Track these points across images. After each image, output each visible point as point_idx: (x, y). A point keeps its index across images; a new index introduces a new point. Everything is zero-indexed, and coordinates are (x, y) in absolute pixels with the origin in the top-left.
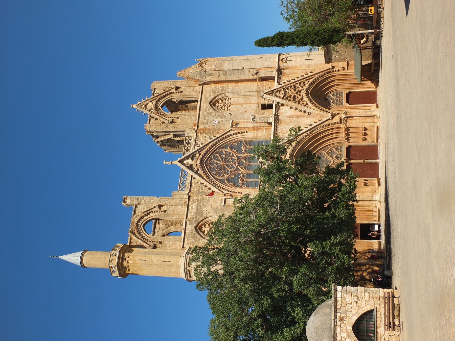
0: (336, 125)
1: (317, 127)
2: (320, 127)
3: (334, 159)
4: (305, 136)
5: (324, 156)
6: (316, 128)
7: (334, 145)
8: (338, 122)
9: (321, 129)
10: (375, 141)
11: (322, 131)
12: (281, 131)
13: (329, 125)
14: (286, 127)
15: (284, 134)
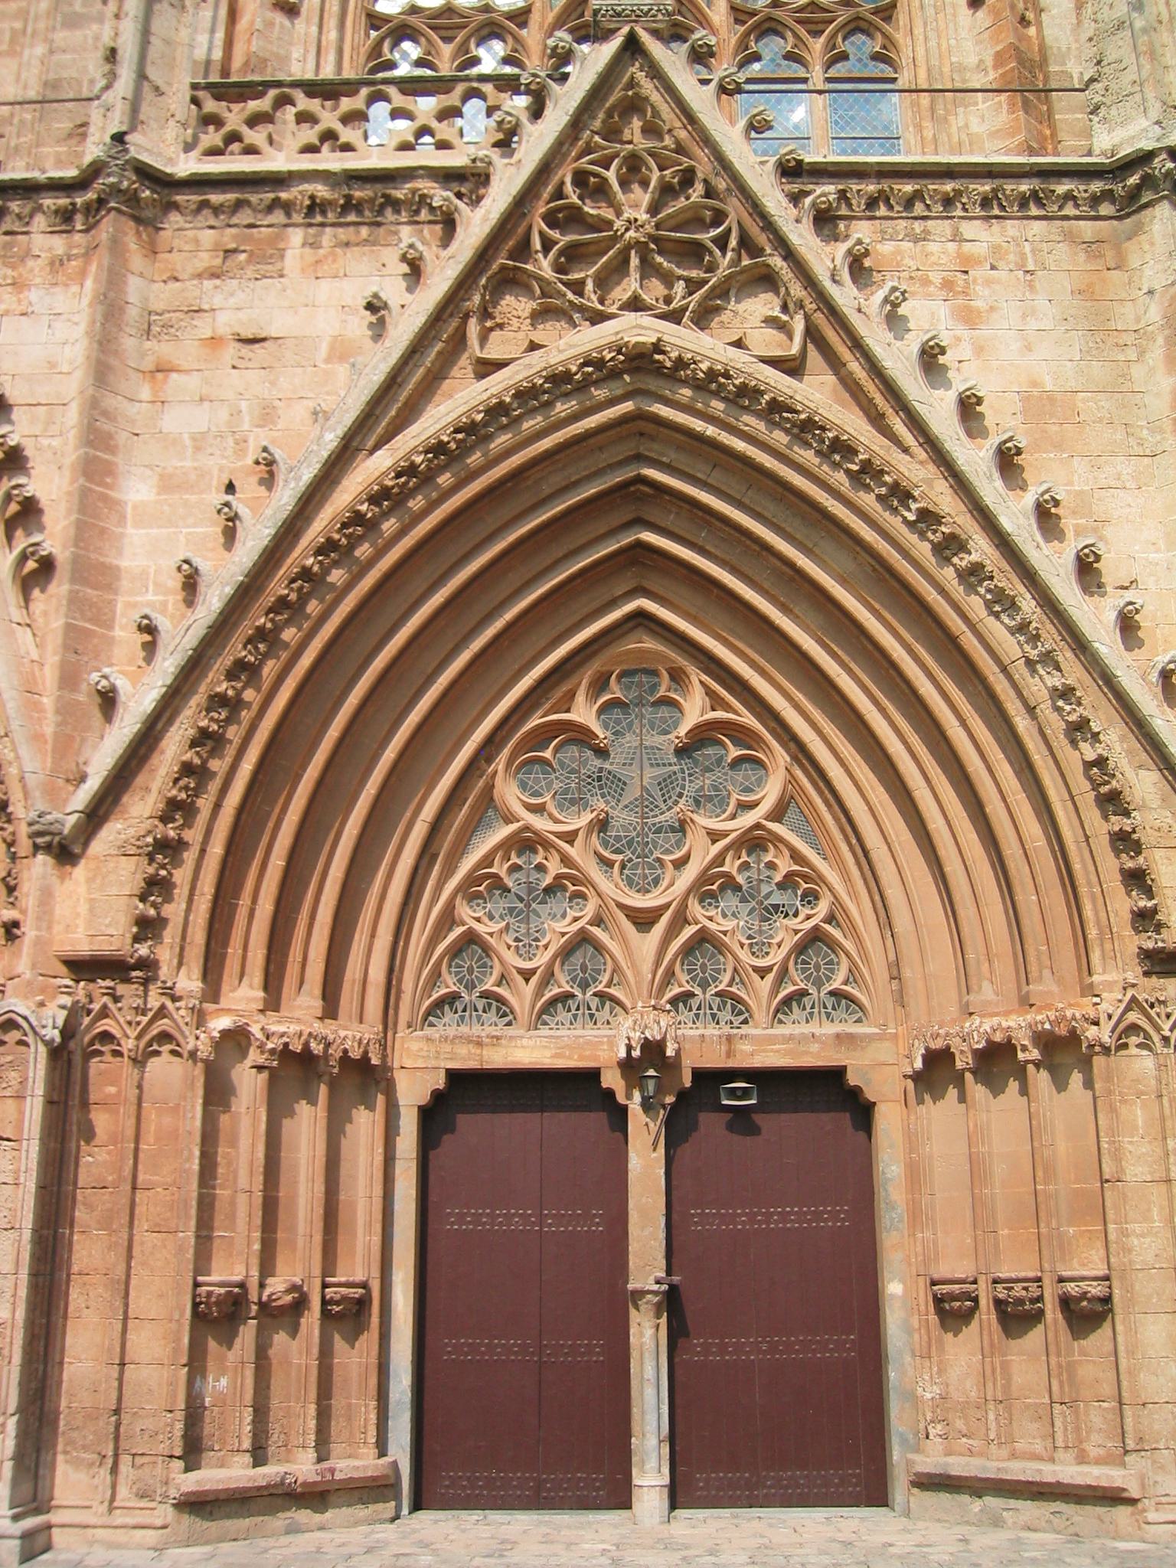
0: (1123, 904)
1: (1066, 657)
2: (1066, 693)
3: (681, 919)
4: (928, 518)
5: (723, 803)
6: (1051, 637)
7: (860, 911)
8: (1159, 927)
9: (1045, 709)
10: (932, 1460)
11: (1022, 724)
12: (979, 249)
13: (1112, 802)
14: (1041, 303)
15: (948, 285)
